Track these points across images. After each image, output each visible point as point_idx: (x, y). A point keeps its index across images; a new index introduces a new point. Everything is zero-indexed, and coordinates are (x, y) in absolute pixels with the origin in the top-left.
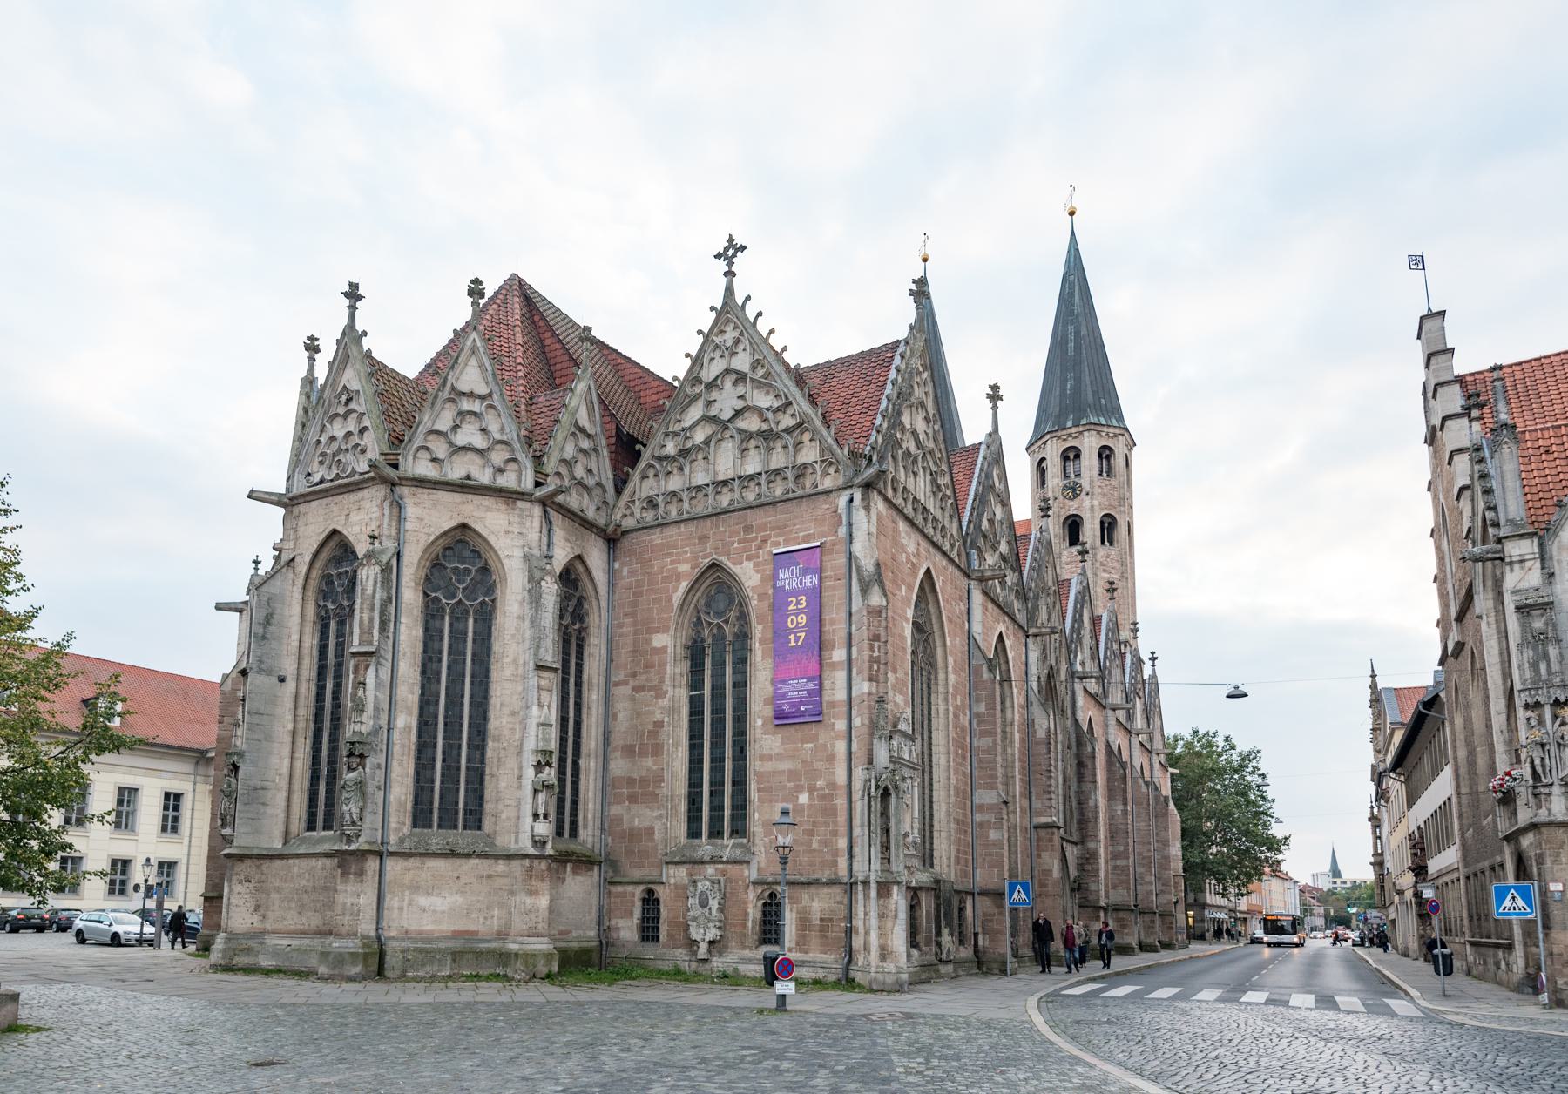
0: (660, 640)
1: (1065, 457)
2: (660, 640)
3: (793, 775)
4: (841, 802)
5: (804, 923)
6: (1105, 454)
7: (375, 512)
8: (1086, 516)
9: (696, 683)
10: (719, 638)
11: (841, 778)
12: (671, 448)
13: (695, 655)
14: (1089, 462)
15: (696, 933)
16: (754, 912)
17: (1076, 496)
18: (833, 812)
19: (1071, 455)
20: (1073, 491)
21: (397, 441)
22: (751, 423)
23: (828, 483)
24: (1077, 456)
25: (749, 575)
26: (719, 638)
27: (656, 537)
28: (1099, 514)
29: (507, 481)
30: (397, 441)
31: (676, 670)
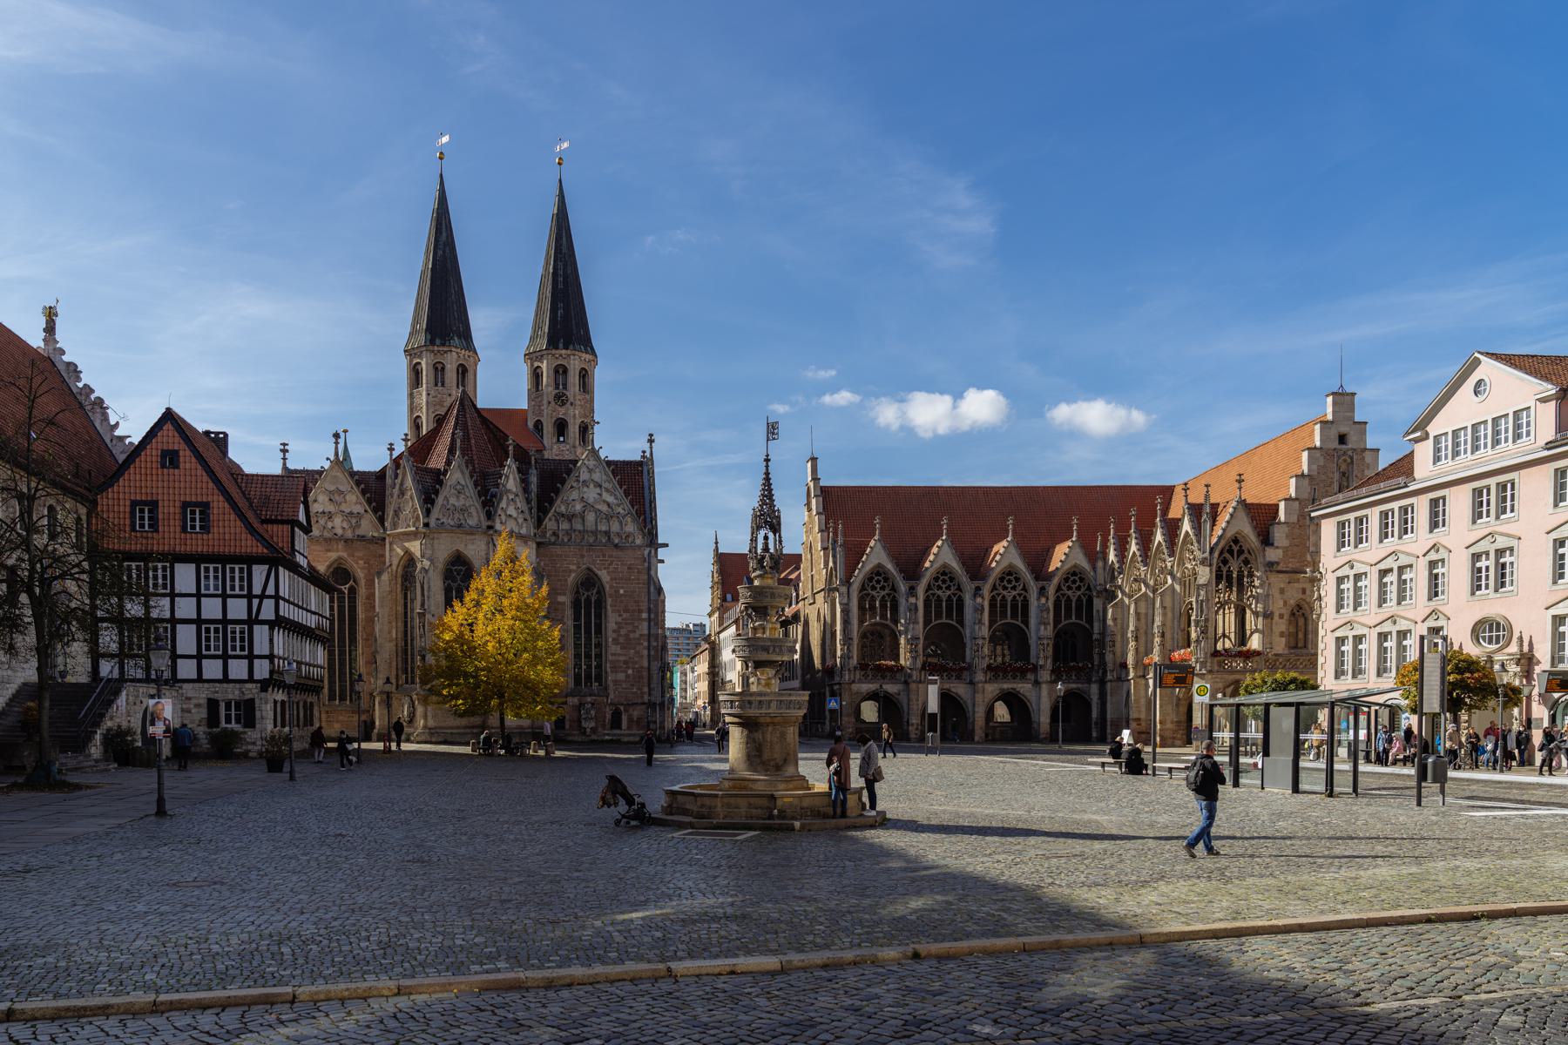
0: (561, 599)
1: (556, 372)
2: (561, 599)
3: (625, 662)
4: (645, 674)
5: (630, 720)
6: (585, 375)
7: (484, 547)
8: (570, 421)
9: (577, 618)
10: (588, 600)
11: (646, 664)
12: (563, 509)
13: (576, 604)
14: (574, 378)
15: (584, 724)
16: (608, 716)
17: (563, 404)
18: (641, 677)
19: (560, 372)
20: (561, 399)
21: (489, 516)
22: (604, 508)
23: (638, 542)
24: (565, 371)
25: (604, 576)
26: (588, 600)
27: (558, 550)
28: (578, 421)
29: (524, 531)
30: (489, 516)
31: (569, 613)
